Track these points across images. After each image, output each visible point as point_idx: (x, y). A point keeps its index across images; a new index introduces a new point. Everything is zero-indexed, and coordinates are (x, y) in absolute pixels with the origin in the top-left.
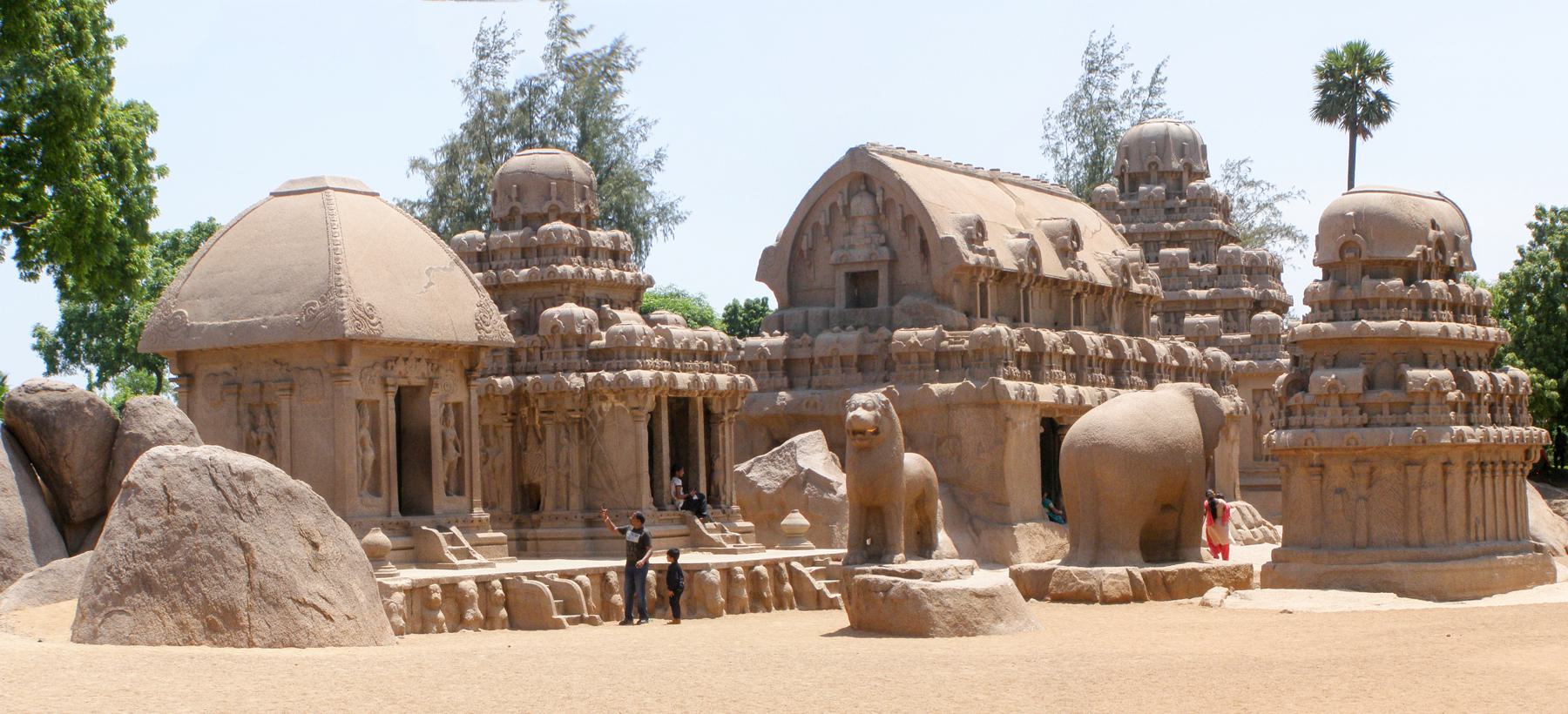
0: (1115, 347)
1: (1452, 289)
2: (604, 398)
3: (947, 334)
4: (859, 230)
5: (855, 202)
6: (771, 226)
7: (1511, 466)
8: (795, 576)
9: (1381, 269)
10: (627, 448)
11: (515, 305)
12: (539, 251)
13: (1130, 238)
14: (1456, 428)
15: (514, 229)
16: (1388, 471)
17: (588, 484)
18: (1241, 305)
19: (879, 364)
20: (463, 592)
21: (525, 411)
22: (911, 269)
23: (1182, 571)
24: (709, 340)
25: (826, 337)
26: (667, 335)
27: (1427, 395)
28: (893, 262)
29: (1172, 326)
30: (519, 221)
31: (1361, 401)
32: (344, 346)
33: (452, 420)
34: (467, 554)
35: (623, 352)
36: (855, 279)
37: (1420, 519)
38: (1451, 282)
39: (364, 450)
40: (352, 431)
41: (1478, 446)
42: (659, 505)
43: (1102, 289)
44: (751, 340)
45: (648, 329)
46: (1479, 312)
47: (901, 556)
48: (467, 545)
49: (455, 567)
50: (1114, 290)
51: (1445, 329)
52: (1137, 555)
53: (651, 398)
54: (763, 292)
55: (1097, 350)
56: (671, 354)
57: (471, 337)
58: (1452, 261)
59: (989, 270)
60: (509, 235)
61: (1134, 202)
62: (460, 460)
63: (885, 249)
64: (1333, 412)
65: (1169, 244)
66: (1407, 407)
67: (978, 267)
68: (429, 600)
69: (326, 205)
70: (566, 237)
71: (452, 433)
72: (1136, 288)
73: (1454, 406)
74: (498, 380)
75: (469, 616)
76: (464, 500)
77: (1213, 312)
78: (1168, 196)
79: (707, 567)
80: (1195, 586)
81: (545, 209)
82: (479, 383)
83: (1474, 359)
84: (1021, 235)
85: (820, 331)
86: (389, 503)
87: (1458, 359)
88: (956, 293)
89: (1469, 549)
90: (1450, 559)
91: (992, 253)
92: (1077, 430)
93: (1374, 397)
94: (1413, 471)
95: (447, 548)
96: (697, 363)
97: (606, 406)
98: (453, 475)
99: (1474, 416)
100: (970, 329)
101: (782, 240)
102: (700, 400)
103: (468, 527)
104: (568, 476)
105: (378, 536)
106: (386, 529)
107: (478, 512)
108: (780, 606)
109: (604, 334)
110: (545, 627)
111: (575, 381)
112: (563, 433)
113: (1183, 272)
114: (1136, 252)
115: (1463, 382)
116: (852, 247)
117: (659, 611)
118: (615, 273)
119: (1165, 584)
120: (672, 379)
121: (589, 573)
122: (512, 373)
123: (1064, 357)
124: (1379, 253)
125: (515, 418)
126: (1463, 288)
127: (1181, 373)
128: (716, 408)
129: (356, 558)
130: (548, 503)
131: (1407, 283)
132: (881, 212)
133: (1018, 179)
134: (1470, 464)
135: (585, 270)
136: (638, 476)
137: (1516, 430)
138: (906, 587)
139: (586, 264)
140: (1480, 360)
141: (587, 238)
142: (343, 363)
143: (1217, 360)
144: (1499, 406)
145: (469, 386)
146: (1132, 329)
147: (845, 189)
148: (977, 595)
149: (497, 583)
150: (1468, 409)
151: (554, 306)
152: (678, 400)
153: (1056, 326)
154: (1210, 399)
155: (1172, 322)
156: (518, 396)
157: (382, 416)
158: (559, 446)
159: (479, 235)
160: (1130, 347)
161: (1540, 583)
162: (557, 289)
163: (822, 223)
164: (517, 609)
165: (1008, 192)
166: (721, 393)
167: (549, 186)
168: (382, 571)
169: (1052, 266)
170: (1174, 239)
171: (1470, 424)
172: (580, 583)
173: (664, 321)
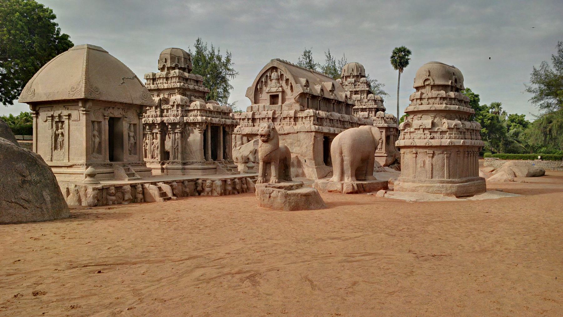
5: (273, 74)
58: (458, 86)
59: (310, 94)
62: (135, 143)
63: (280, 88)
67: (307, 93)
71: (132, 134)
80: (372, 189)
81: (173, 65)
101: (253, 86)
118: (196, 87)
149: (140, 186)
157: (103, 127)
160: (347, 117)
172: (171, 186)
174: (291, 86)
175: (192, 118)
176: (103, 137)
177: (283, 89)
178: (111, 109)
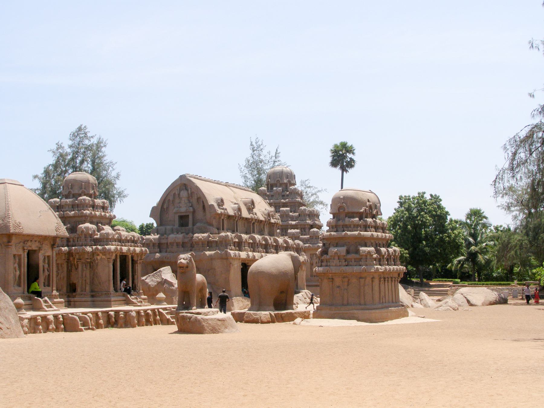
0: (266, 240)
1: (375, 222)
2: (98, 255)
3: (211, 236)
4: (183, 202)
5: (182, 192)
6: (155, 199)
7: (394, 279)
8: (160, 314)
9: (351, 215)
10: (105, 272)
11: (69, 223)
12: (78, 206)
13: (270, 205)
14: (376, 267)
15: (70, 198)
16: (354, 280)
17: (92, 283)
18: (306, 226)
19: (189, 245)
20: (48, 319)
21: (71, 258)
22: (200, 214)
23: (287, 313)
24: (134, 236)
25: (172, 236)
26: (120, 234)
27: (366, 256)
28: (194, 212)
29: (284, 233)
30: (71, 196)
31: (345, 258)
32: (10, 236)
33: (47, 261)
34: (50, 307)
35: (105, 240)
36: (181, 217)
37: (364, 296)
38: (374, 219)
39: (16, 271)
40: (11, 265)
41: (383, 272)
42: (116, 290)
43: (261, 221)
44: (148, 237)
45: (114, 232)
46: (383, 229)
47: (195, 307)
48: (50, 303)
49: (46, 311)
50: (265, 221)
51: (372, 235)
52: (272, 308)
53: (114, 255)
54: (152, 221)
55: (260, 241)
56: (121, 241)
57: (54, 234)
58: (374, 212)
59: (225, 215)
60: (68, 200)
61: (272, 193)
62: (49, 275)
63: (191, 208)
64: (336, 261)
65: (283, 207)
66: (360, 259)
67: (221, 214)
68: (37, 322)
69: (5, 188)
70: (87, 201)
71: (46, 266)
72: (273, 221)
73: (375, 259)
74: (63, 248)
75: (50, 327)
76: (50, 288)
77: (297, 229)
78: (283, 191)
79: (131, 311)
80: (291, 318)
81: (80, 192)
82: (56, 249)
83: (382, 244)
84: (235, 204)
85: (170, 234)
86: (24, 288)
87: (376, 244)
88: (214, 222)
89: (380, 306)
90: (374, 309)
91: (226, 209)
92: (253, 267)
93: (349, 256)
94: (362, 281)
95: (44, 305)
96: (129, 244)
97: (99, 258)
98: (46, 281)
99: (382, 263)
100: (219, 234)
101: (158, 204)
102: (130, 256)
103: (51, 297)
104: (86, 280)
105: (20, 301)
106: (23, 298)
107: (55, 292)
108: (155, 324)
109: (99, 234)
110: (77, 331)
111: (89, 249)
112: (84, 266)
113: (287, 216)
114: (273, 209)
115: (378, 252)
116: (180, 207)
117: (115, 326)
118: (103, 214)
119: (281, 317)
120: (121, 249)
121: (92, 313)
122: (68, 246)
123: (249, 243)
124: (351, 210)
125: (68, 261)
126: (378, 221)
127: (287, 249)
128: (135, 258)
129: (11, 308)
130: (79, 290)
131: (360, 220)
132: (190, 197)
133: (234, 186)
134: (380, 278)
135: (93, 212)
136: (109, 280)
137: (395, 267)
138: (196, 317)
139: (93, 210)
140: (383, 244)
141: (94, 202)
142: (9, 242)
143: (299, 244)
144: (390, 259)
145: (52, 250)
146: (271, 234)
147: (178, 188)
148: (219, 320)
149: (60, 316)
150: (380, 260)
151: (82, 224)
152: (123, 256)
153: (246, 233)
154: (296, 257)
155: (284, 231)
156: (70, 253)
157: (22, 260)
158: (83, 270)
159: (58, 200)
161: (404, 317)
162: (84, 218)
163: (171, 199)
164: (67, 325)
165: (231, 190)
166: (137, 254)
167: (82, 185)
168: (21, 312)
169: (245, 214)
170: (285, 205)
171: (380, 265)
172: (89, 316)
173: (119, 230)
175: (100, 247)
177: (194, 209)
178: (29, 241)
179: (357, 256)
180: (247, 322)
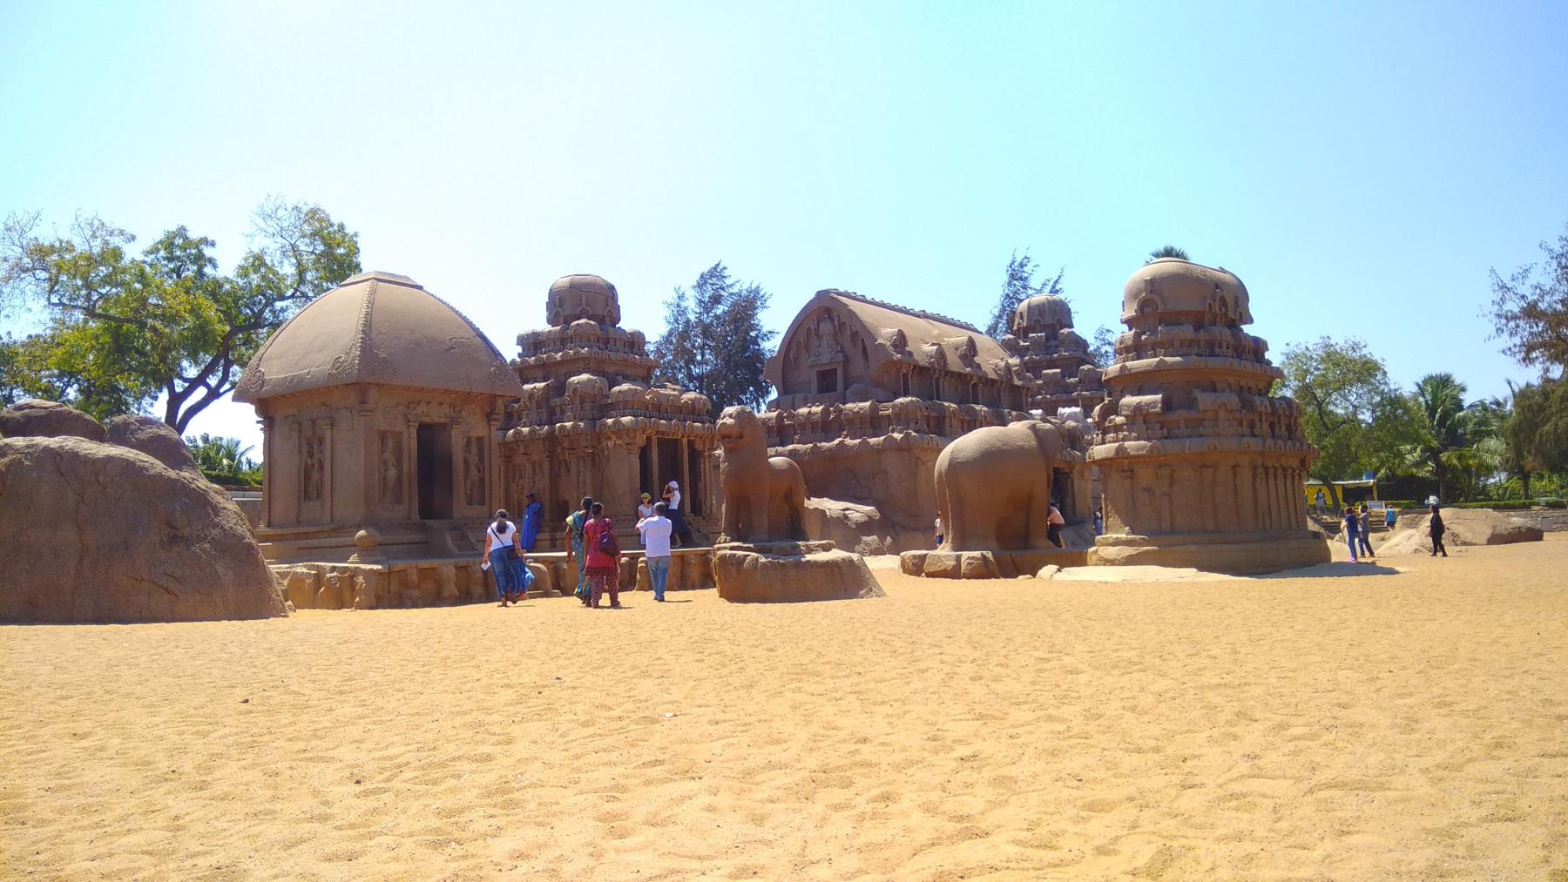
4: (824, 344)
22: (858, 367)
25: (804, 410)
28: (847, 361)
33: (474, 450)
43: (993, 381)
66: (1201, 422)
71: (474, 459)
72: (1017, 382)
76: (485, 509)
93: (1170, 416)
97: (610, 444)
125: (552, 455)
128: (699, 446)
134: (1255, 468)
169: (954, 363)
174: (864, 349)
176: (405, 465)
179: (1193, 414)
180: (931, 575)
